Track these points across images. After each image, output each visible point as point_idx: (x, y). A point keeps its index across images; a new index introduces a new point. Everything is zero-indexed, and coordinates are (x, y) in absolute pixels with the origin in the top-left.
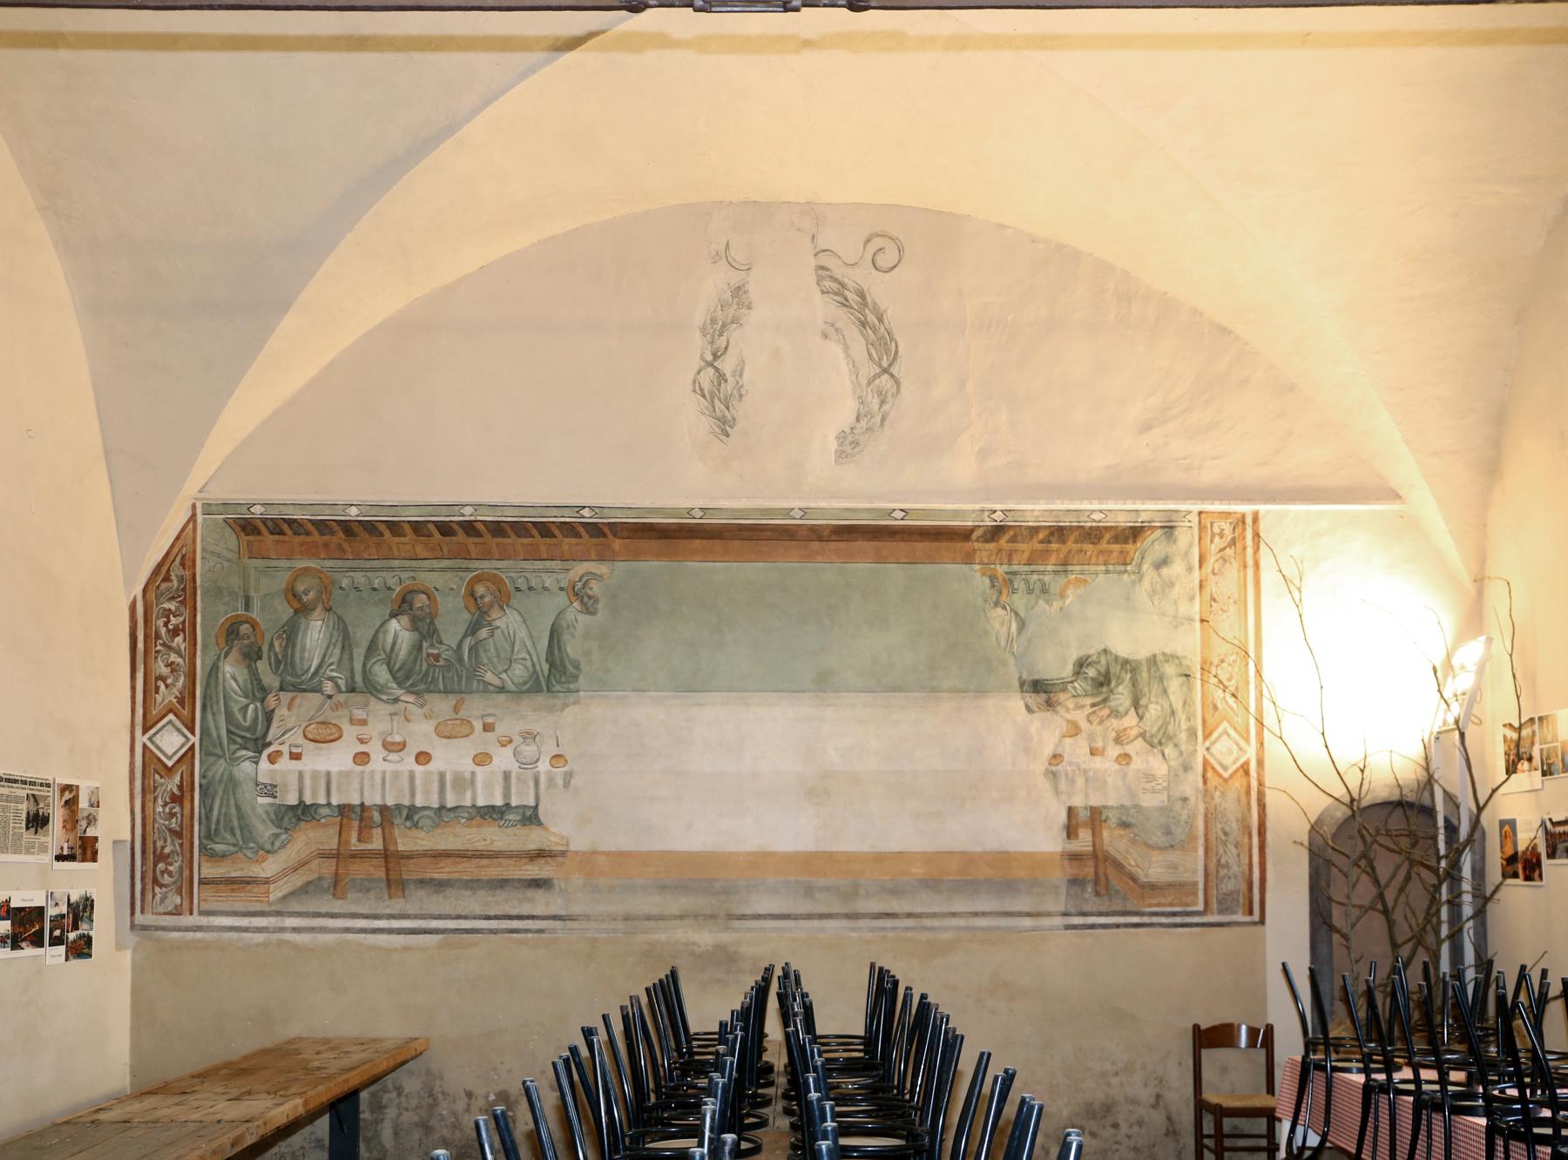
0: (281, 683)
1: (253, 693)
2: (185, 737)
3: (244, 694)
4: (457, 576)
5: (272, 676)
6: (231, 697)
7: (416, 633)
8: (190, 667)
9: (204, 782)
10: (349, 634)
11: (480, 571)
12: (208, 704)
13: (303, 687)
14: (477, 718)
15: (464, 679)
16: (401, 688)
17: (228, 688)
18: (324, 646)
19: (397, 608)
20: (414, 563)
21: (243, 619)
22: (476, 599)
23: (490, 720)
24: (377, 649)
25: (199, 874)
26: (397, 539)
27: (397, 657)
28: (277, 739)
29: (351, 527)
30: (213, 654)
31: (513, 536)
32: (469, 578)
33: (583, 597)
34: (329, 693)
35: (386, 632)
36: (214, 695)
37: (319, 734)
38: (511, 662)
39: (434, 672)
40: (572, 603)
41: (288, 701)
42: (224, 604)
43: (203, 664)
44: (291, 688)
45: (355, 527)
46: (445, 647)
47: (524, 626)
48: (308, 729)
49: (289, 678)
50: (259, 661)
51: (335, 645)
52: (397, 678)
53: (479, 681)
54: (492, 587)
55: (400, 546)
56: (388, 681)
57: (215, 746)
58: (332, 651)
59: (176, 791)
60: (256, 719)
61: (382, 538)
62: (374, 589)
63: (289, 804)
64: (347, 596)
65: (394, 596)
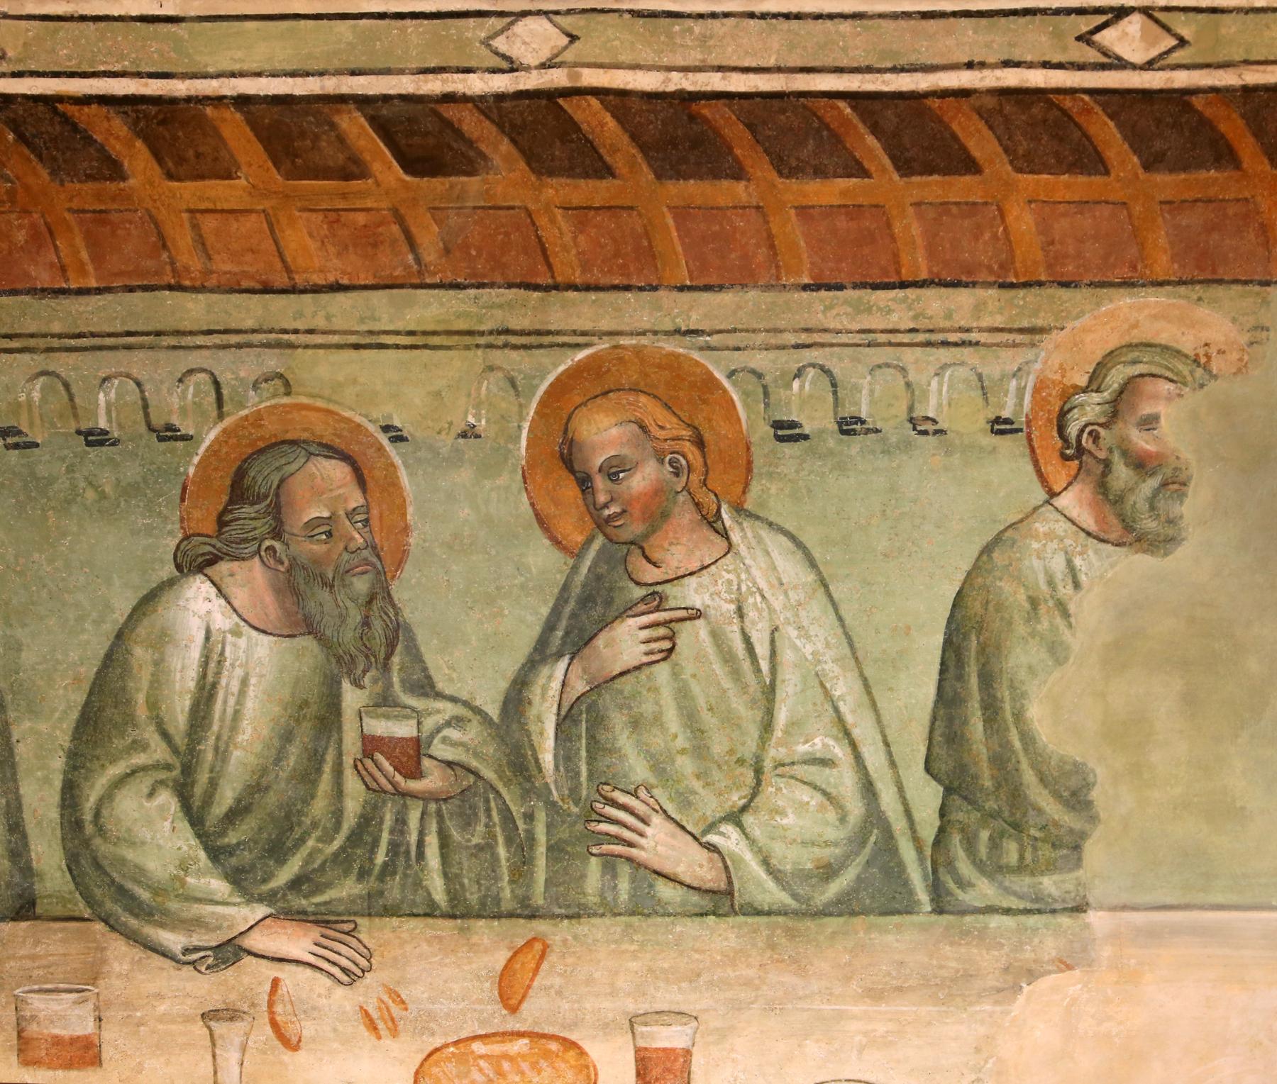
4: (491, 368)
7: (308, 642)
11: (603, 345)
14: (606, 1027)
15: (541, 850)
19: (210, 527)
20: (282, 310)
22: (585, 483)
23: (669, 1037)
24: (130, 720)
26: (188, 192)
27: (222, 754)
31: (762, 169)
32: (551, 378)
33: (1107, 464)
35: (163, 640)
38: (758, 771)
39: (401, 821)
40: (1053, 494)
46: (449, 709)
47: (817, 607)
53: (610, 863)
54: (667, 425)
55: (209, 224)
61: (111, 186)
62: (96, 438)
65: (191, 470)
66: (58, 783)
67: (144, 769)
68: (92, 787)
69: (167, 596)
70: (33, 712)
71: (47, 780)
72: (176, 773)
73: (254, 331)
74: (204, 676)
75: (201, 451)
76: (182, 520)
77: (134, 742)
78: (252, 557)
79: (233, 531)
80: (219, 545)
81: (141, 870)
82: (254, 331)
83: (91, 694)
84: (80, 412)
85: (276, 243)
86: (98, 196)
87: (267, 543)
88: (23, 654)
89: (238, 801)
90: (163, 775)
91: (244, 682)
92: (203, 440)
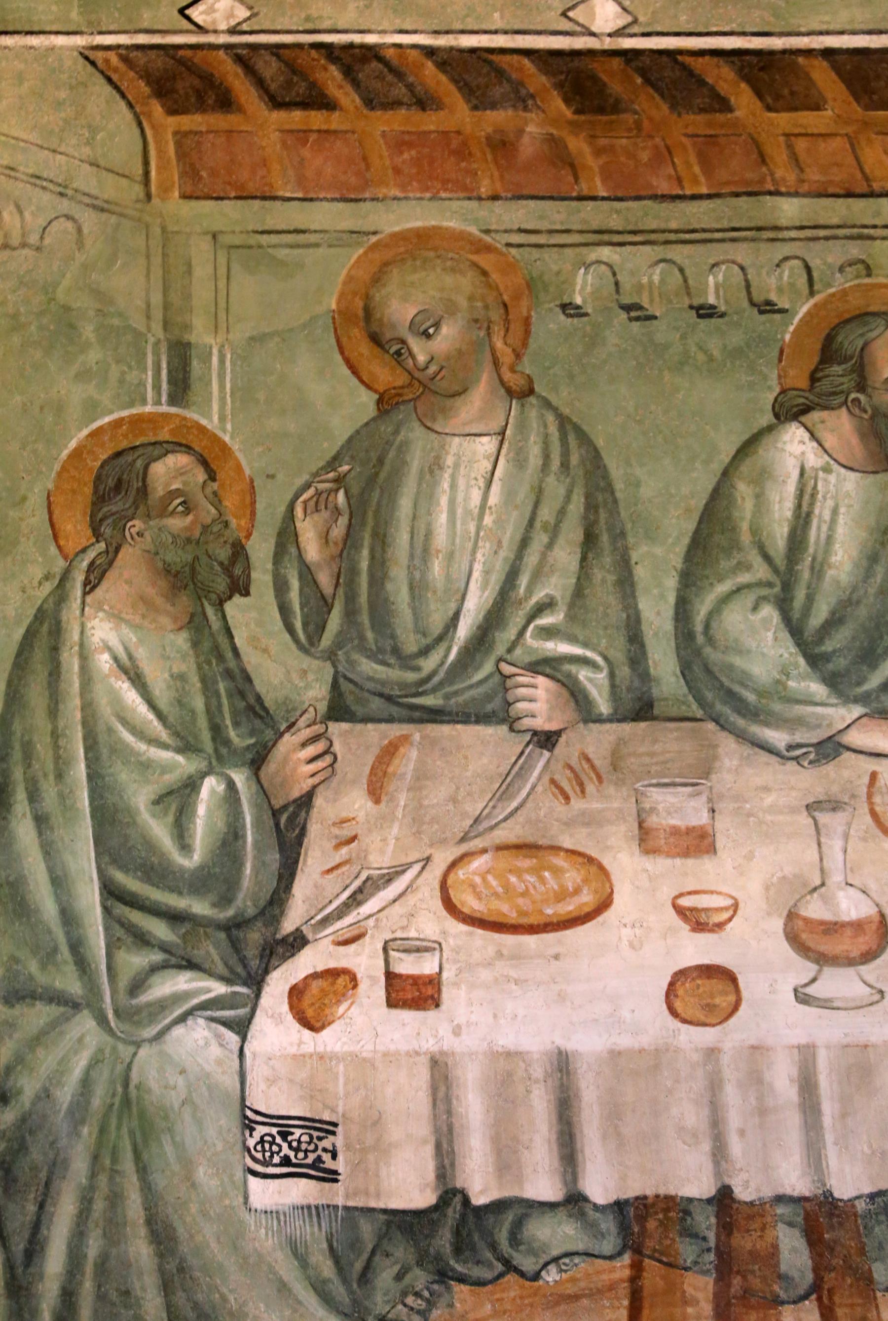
0: (335, 685)
6: (119, 750)
13: (428, 701)
17: (105, 710)
18: (510, 534)
19: (804, 383)
21: (164, 435)
24: (735, 545)
26: (783, 120)
28: (326, 921)
29: (594, 78)
34: (540, 723)
36: (42, 748)
41: (370, 759)
48: (461, 873)
49: (368, 667)
51: (554, 531)
52: (826, 658)
55: (801, 145)
61: (720, 117)
65: (788, 337)
66: (672, 599)
67: (748, 586)
68: (702, 602)
69: (766, 440)
71: (662, 596)
72: (777, 589)
73: (839, 227)
74: (799, 506)
75: (796, 321)
76: (780, 377)
77: (739, 563)
78: (840, 407)
79: (824, 386)
80: (811, 397)
82: (839, 227)
83: (700, 522)
85: (857, 159)
87: (853, 396)
89: (833, 613)
90: (765, 592)
91: (835, 512)
92: (797, 313)
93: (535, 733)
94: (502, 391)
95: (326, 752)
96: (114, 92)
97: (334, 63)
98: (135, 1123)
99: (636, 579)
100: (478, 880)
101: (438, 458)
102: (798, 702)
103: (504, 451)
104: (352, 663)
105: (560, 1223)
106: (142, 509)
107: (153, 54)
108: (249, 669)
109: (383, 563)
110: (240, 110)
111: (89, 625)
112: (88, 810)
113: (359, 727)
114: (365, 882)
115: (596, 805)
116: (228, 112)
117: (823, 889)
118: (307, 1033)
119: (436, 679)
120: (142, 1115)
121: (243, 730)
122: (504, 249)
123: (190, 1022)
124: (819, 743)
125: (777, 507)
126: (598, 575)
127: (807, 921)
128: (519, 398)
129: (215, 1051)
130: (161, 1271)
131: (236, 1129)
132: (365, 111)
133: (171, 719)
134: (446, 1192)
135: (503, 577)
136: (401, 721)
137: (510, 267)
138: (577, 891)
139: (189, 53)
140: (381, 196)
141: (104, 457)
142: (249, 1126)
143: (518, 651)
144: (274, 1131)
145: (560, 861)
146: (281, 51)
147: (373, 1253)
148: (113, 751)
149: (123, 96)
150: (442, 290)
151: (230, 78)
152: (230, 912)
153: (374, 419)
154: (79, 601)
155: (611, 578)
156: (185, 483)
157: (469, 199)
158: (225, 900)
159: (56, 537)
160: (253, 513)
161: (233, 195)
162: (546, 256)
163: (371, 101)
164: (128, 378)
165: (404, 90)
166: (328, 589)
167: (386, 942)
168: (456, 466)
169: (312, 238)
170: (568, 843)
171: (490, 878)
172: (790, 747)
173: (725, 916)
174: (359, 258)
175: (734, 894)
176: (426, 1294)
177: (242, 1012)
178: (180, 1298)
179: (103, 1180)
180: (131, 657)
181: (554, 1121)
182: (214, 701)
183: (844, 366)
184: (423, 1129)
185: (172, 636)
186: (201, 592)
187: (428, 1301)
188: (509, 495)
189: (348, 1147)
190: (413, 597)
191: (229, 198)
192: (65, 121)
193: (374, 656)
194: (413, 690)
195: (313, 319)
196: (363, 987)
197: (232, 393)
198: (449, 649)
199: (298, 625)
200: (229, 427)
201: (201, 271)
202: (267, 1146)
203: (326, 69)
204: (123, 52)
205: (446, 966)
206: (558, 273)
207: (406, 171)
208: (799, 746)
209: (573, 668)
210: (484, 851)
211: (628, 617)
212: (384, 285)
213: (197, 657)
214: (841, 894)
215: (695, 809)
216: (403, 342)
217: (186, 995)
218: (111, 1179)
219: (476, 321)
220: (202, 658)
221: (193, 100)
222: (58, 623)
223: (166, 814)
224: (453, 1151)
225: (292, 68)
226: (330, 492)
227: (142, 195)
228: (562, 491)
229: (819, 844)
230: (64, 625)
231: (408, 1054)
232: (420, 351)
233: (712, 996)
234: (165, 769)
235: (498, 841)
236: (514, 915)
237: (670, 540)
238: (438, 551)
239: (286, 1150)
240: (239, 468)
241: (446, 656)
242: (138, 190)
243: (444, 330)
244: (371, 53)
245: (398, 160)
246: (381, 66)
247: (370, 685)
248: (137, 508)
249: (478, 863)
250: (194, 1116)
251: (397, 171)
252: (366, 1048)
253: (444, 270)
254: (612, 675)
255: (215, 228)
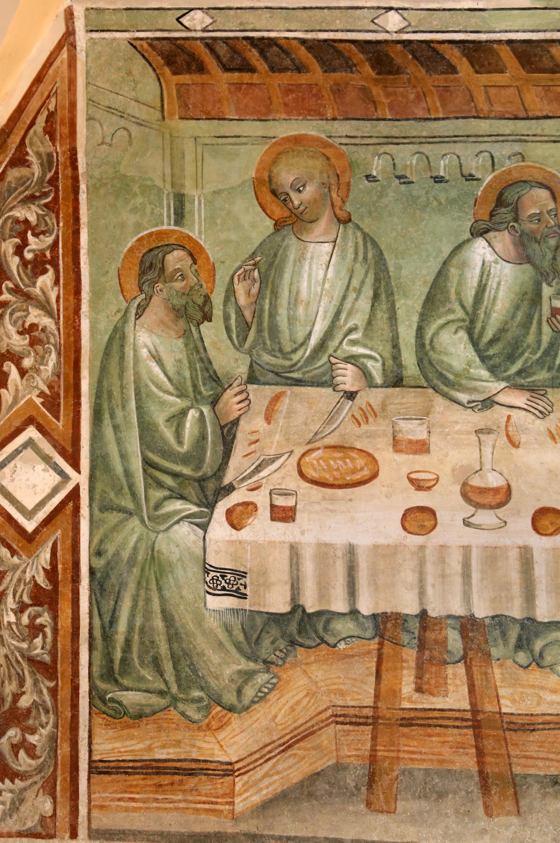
0: (251, 366)
1: (195, 386)
2: (61, 473)
3: (177, 389)
5: (232, 353)
6: (150, 395)
8: (67, 336)
9: (100, 563)
10: (387, 270)
12: (105, 405)
13: (295, 375)
16: (499, 379)
17: (145, 377)
18: (337, 294)
21: (172, 241)
24: (448, 300)
25: (90, 751)
28: (244, 479)
30: (113, 308)
36: (116, 393)
37: (330, 469)
41: (266, 403)
42: (134, 210)
43: (93, 330)
44: (271, 375)
45: (396, 54)
48: (307, 459)
49: (267, 358)
50: (206, 323)
51: (359, 292)
52: (490, 358)
56: (469, 364)
57: (119, 491)
58: (354, 304)
59: (41, 580)
60: (203, 437)
63: (272, 610)
64: (381, 195)
66: (415, 327)
67: (453, 321)
68: (430, 329)
70: (405, 296)
72: (467, 323)
77: (449, 309)
81: (450, 366)
84: (432, 169)
86: (446, 80)
88: (403, 271)
90: (461, 324)
93: (345, 392)
94: (336, 220)
95: (246, 399)
96: (146, 63)
97: (255, 48)
98: (157, 568)
99: (398, 316)
100: (315, 462)
101: (303, 254)
102: (475, 380)
103: (335, 251)
104: (259, 355)
105: (347, 623)
106: (162, 278)
107: (165, 42)
108: (211, 358)
109: (275, 307)
110: (208, 72)
111: (138, 335)
112: (136, 423)
113: (262, 387)
114: (262, 462)
115: (373, 428)
116: (202, 73)
117: (481, 472)
118: (234, 531)
119: (299, 365)
120: (160, 564)
121: (208, 387)
122: (338, 146)
123: (181, 523)
124: (484, 400)
125: (470, 281)
126: (379, 314)
127: (471, 487)
128: (343, 224)
129: (192, 537)
130: (168, 634)
131: (201, 573)
132: (270, 73)
133: (174, 381)
134: (295, 606)
135: (333, 315)
136: (282, 384)
137: (341, 155)
138: (362, 469)
139: (182, 42)
140: (277, 118)
141: (144, 251)
142: (207, 572)
143: (339, 352)
144: (218, 574)
145: (353, 454)
146: (228, 41)
147: (262, 631)
148: (148, 396)
149: (151, 65)
150: (307, 167)
151: (203, 56)
152: (200, 474)
153: (272, 234)
154: (133, 323)
155: (386, 316)
156: (182, 265)
157: (322, 120)
158: (198, 468)
159: (122, 291)
160: (214, 281)
161: (204, 117)
162: (359, 150)
163: (273, 68)
164: (155, 211)
165: (290, 62)
166: (249, 319)
167: (271, 490)
168: (312, 258)
169: (244, 140)
170: (358, 445)
171: (321, 461)
172: (469, 402)
173: (433, 483)
174: (266, 150)
175: (437, 473)
176: (285, 651)
177: (204, 520)
178: (175, 646)
179: (142, 592)
180: (156, 351)
181: (346, 576)
182: (194, 373)
183: (507, 209)
184: (285, 576)
185: (176, 341)
186: (189, 319)
187: (285, 654)
188: (337, 272)
189: (252, 583)
190: (289, 324)
191: (202, 119)
192: (123, 78)
193: (271, 353)
194: (288, 370)
195: (244, 182)
196: (260, 511)
197: (205, 220)
198: (306, 350)
199: (234, 337)
200: (203, 237)
201: (189, 157)
202: (215, 581)
203: (250, 51)
204: (150, 41)
205: (299, 502)
206: (365, 159)
207: (290, 105)
208: (474, 401)
209: (365, 361)
210: (319, 448)
211: (393, 336)
212: (278, 165)
213: (187, 351)
214: (489, 474)
215: (420, 431)
216: (288, 194)
217: (180, 511)
218: (146, 592)
219: (323, 184)
220: (189, 352)
221: (185, 67)
222: (124, 333)
223: (172, 426)
224: (299, 588)
225: (234, 50)
226: (251, 270)
227: (160, 117)
228: (363, 272)
229: (480, 450)
230: (126, 334)
231: (280, 542)
232: (296, 199)
233: (423, 521)
234: (171, 405)
235: (325, 444)
236: (332, 479)
237: (416, 297)
238: (302, 301)
239: (223, 583)
240: (208, 258)
241: (304, 353)
242: (158, 115)
243: (308, 188)
244: (272, 42)
245: (286, 99)
246: (278, 49)
247: (267, 367)
248: (160, 277)
249: (315, 454)
250: (182, 566)
251: (286, 105)
252: (261, 539)
253: (308, 157)
254: (384, 364)
255: (196, 135)
